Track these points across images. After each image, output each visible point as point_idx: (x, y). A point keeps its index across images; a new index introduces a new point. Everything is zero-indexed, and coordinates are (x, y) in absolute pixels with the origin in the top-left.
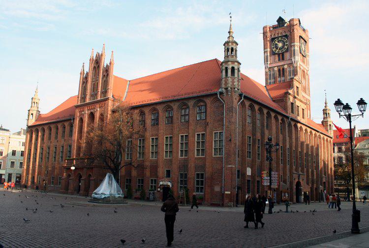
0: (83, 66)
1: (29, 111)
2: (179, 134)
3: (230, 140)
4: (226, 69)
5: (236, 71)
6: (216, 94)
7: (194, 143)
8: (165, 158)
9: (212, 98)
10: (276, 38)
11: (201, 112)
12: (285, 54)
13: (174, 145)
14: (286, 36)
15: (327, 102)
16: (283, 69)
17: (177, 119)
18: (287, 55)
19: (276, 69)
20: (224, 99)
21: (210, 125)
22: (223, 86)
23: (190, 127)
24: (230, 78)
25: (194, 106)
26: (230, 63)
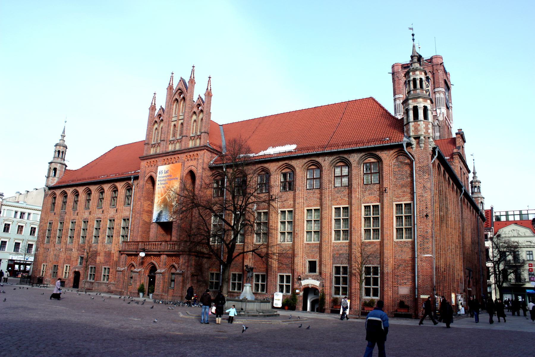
0: (154, 98)
1: (50, 163)
2: (332, 205)
3: (427, 216)
4: (415, 109)
5: (429, 113)
6: (402, 145)
7: (361, 220)
8: (305, 242)
11: (371, 173)
13: (325, 222)
15: (476, 171)
17: (330, 181)
20: (413, 153)
22: (412, 134)
23: (353, 195)
24: (422, 122)
25: (359, 163)
26: (421, 100)
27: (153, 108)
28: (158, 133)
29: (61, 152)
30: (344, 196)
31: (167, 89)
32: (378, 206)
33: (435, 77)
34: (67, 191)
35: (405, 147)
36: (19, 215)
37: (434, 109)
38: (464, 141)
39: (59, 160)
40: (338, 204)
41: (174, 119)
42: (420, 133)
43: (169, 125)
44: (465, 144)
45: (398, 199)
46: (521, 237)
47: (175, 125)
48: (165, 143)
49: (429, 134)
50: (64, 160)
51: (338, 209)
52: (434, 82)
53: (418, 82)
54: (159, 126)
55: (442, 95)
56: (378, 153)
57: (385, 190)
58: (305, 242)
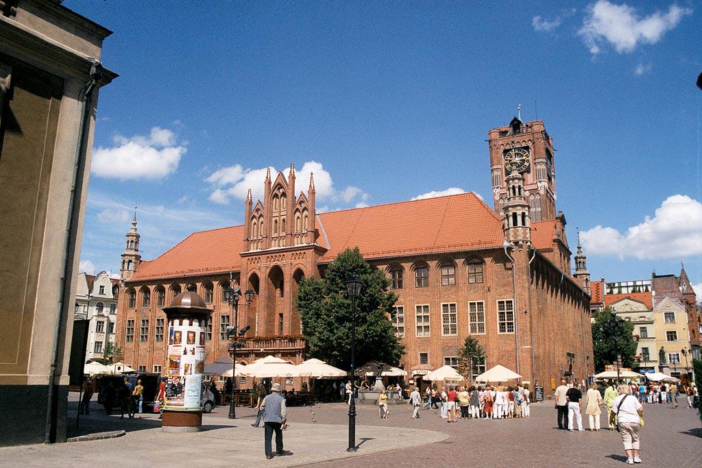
2: (440, 302)
3: (526, 312)
4: (515, 215)
5: (527, 218)
7: (467, 316)
14: (527, 148)
20: (513, 256)
22: (512, 239)
28: (258, 228)
30: (452, 294)
31: (265, 183)
37: (535, 182)
43: (271, 221)
52: (535, 152)
53: (517, 190)
54: (258, 221)
55: (544, 167)
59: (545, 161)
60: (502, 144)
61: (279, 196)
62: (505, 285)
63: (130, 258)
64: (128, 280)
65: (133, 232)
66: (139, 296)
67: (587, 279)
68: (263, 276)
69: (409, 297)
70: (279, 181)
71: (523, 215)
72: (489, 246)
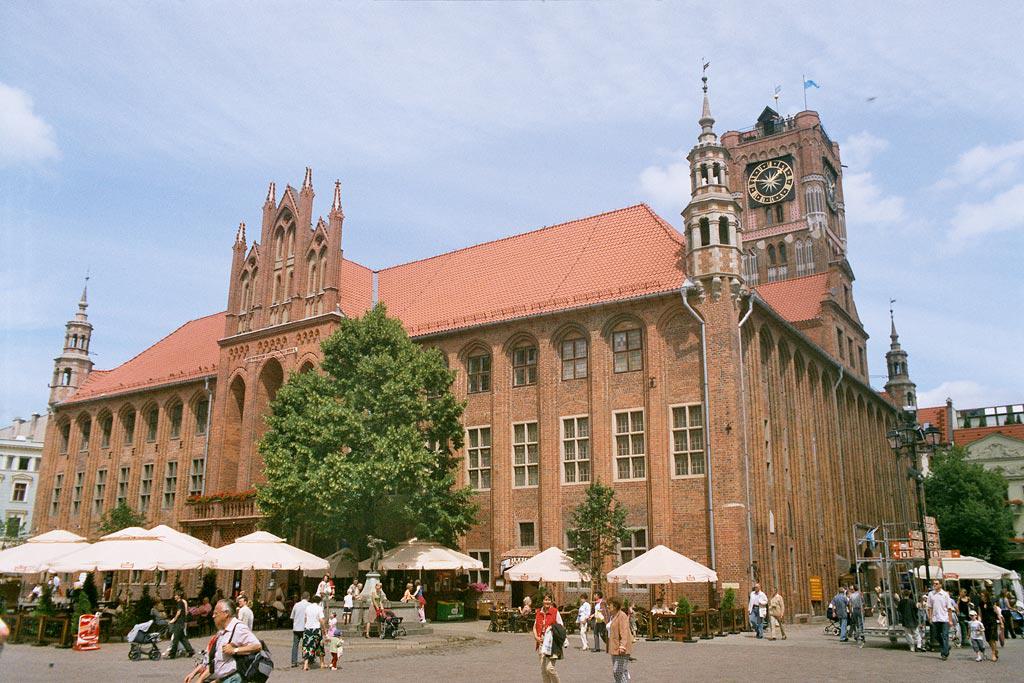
1: (58, 360)
2: (558, 414)
3: (729, 429)
4: (704, 225)
5: (732, 230)
8: (514, 487)
9: (663, 309)
10: (758, 163)
12: (786, 206)
13: (545, 449)
14: (788, 158)
16: (782, 246)
18: (793, 210)
19: (762, 245)
21: (660, 387)
22: (698, 272)
27: (240, 248)
29: (80, 334)
31: (264, 208)
32: (641, 412)
33: (805, 156)
34: (91, 413)
35: (685, 299)
36: (16, 463)
38: (851, 278)
39: (76, 355)
40: (569, 413)
41: (278, 266)
42: (712, 270)
44: (853, 283)
45: (678, 399)
46: (1011, 459)
47: (279, 277)
48: (262, 311)
49: (731, 270)
50: (87, 353)
51: (569, 423)
52: (802, 164)
55: (818, 189)
56: (638, 312)
57: (652, 383)
58: (514, 487)
59: (821, 179)
60: (744, 156)
61: (286, 230)
62: (685, 373)
63: (68, 365)
64: (61, 402)
65: (78, 319)
66: (75, 432)
67: (909, 394)
68: (251, 379)
69: (496, 409)
70: (286, 202)
71: (723, 224)
72: (651, 292)
